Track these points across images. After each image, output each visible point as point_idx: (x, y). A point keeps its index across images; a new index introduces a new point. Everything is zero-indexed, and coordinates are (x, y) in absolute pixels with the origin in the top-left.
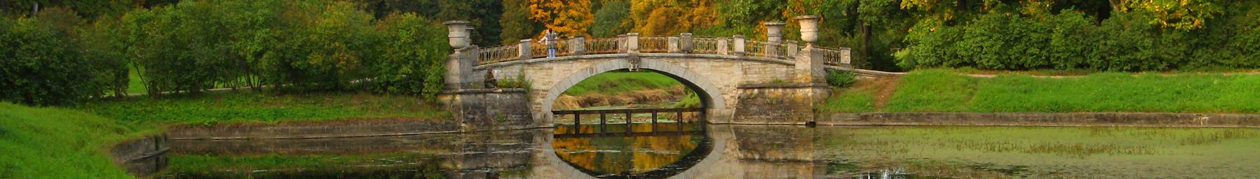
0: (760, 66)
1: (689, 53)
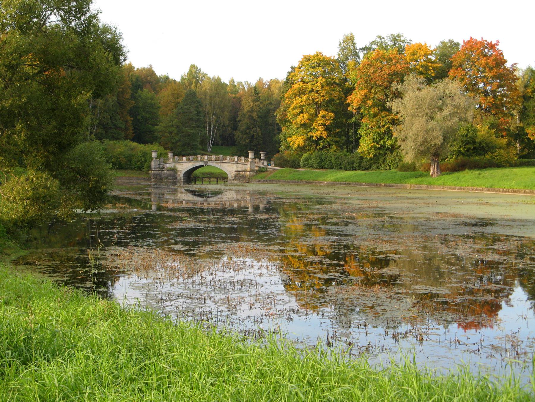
1: (222, 161)
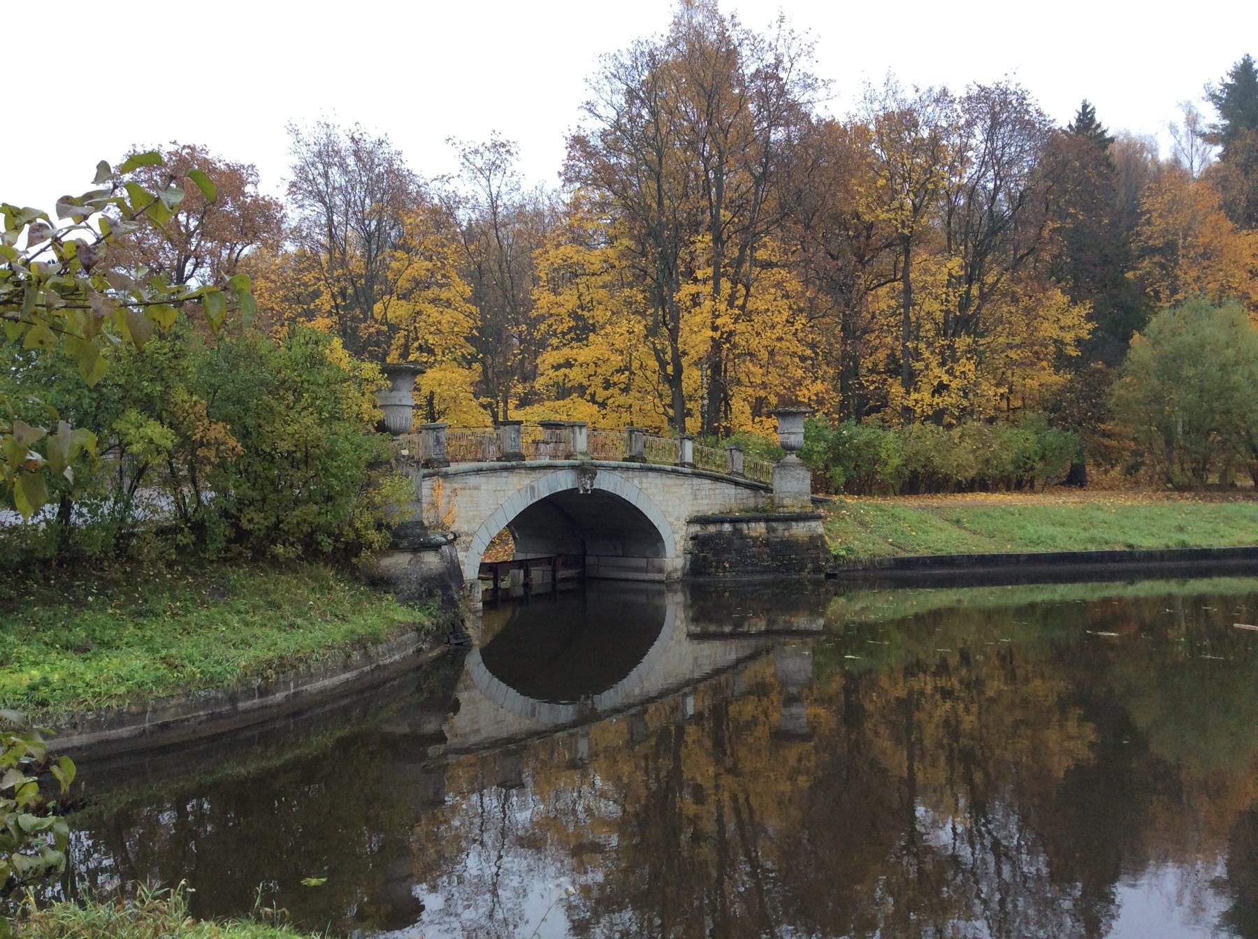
0: (710, 487)
